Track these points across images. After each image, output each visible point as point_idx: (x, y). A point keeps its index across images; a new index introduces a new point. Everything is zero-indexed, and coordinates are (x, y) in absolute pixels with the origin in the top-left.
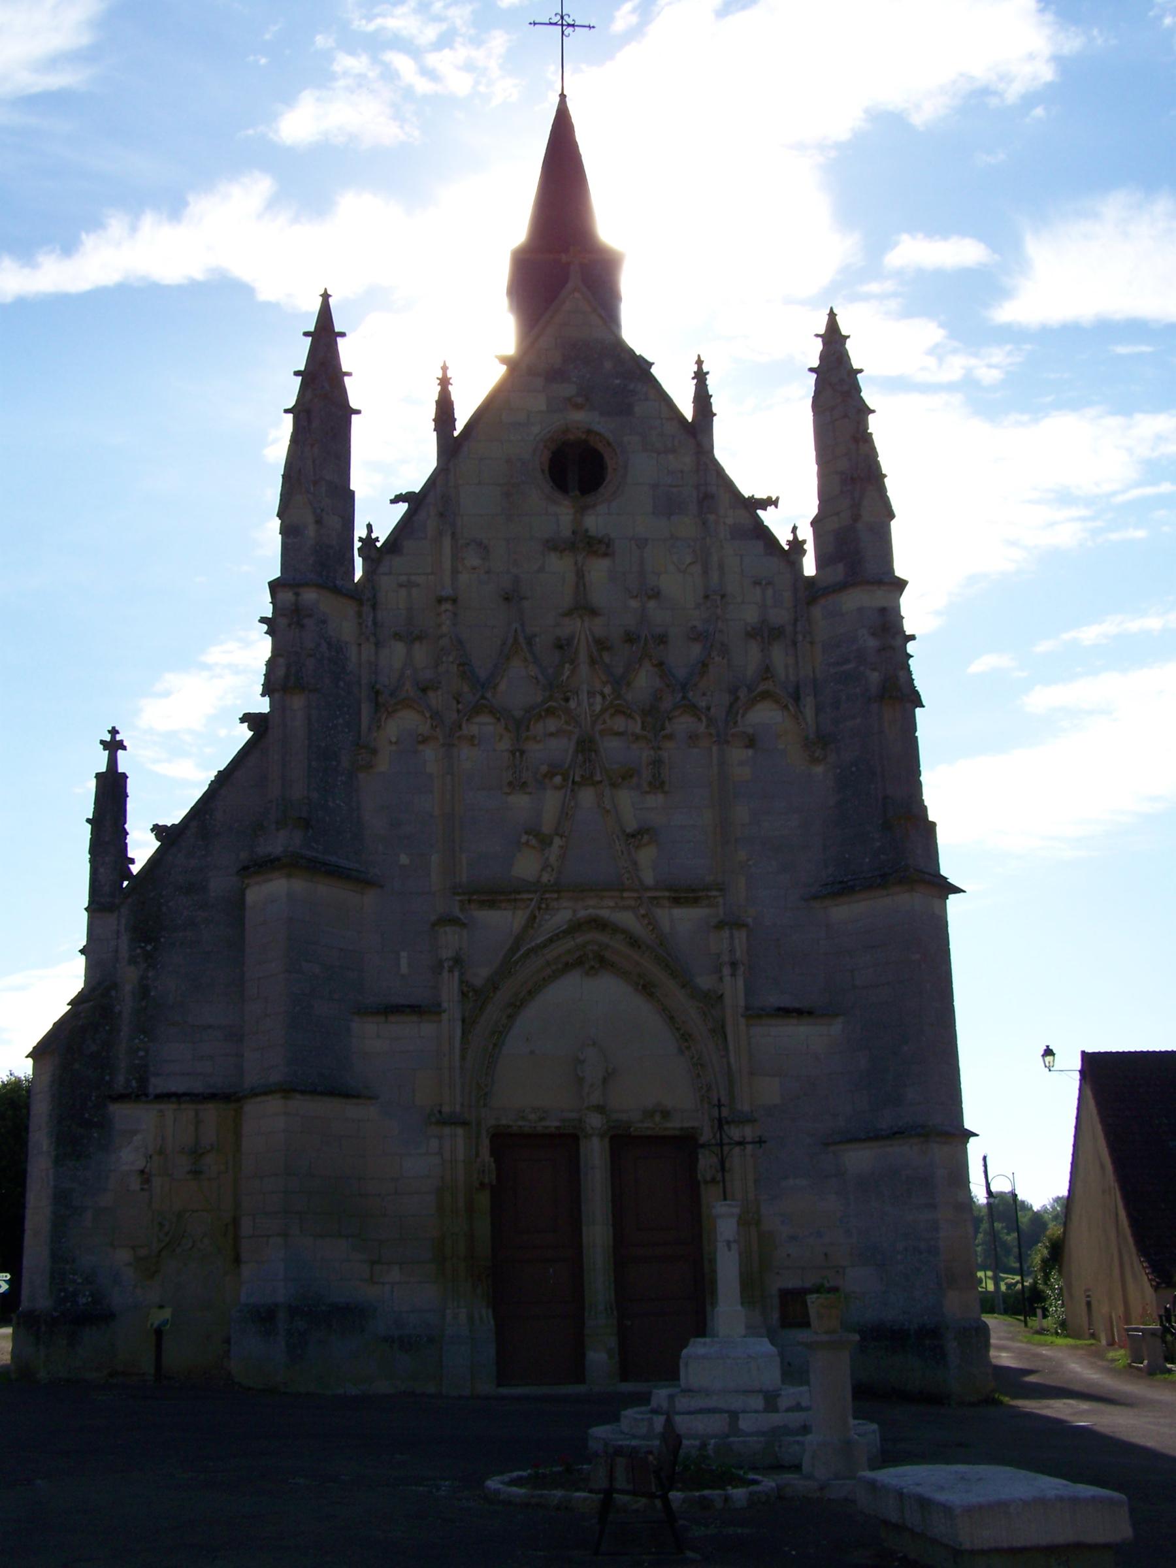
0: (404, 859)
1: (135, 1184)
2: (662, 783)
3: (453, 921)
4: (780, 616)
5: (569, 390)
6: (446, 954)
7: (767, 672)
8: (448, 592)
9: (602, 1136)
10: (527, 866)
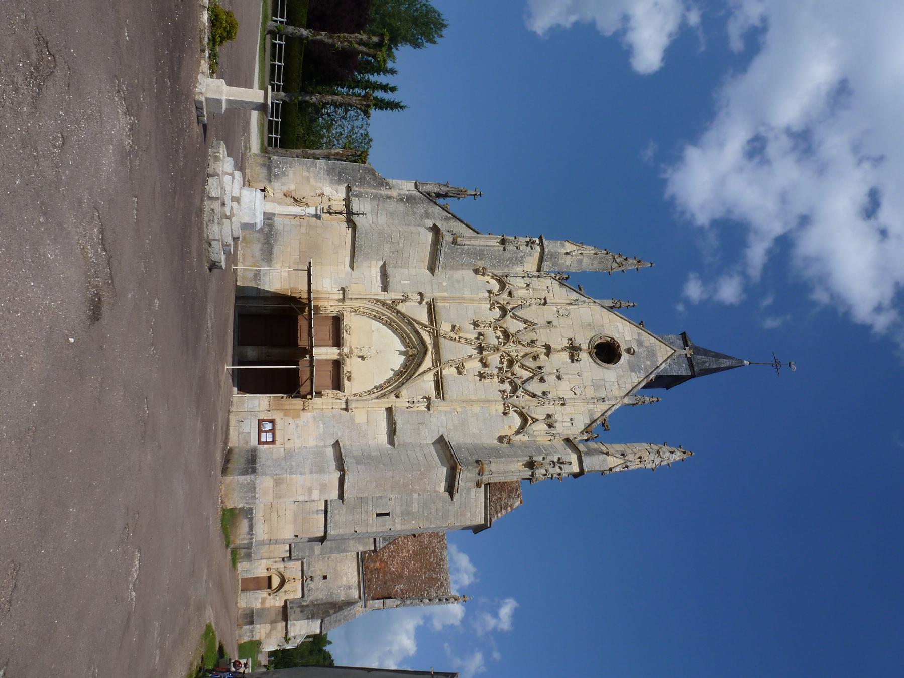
0: (445, 284)
1: (319, 192)
2: (485, 377)
3: (422, 299)
5: (636, 348)
6: (410, 294)
7: (535, 421)
8: (548, 301)
9: (340, 354)
10: (445, 328)
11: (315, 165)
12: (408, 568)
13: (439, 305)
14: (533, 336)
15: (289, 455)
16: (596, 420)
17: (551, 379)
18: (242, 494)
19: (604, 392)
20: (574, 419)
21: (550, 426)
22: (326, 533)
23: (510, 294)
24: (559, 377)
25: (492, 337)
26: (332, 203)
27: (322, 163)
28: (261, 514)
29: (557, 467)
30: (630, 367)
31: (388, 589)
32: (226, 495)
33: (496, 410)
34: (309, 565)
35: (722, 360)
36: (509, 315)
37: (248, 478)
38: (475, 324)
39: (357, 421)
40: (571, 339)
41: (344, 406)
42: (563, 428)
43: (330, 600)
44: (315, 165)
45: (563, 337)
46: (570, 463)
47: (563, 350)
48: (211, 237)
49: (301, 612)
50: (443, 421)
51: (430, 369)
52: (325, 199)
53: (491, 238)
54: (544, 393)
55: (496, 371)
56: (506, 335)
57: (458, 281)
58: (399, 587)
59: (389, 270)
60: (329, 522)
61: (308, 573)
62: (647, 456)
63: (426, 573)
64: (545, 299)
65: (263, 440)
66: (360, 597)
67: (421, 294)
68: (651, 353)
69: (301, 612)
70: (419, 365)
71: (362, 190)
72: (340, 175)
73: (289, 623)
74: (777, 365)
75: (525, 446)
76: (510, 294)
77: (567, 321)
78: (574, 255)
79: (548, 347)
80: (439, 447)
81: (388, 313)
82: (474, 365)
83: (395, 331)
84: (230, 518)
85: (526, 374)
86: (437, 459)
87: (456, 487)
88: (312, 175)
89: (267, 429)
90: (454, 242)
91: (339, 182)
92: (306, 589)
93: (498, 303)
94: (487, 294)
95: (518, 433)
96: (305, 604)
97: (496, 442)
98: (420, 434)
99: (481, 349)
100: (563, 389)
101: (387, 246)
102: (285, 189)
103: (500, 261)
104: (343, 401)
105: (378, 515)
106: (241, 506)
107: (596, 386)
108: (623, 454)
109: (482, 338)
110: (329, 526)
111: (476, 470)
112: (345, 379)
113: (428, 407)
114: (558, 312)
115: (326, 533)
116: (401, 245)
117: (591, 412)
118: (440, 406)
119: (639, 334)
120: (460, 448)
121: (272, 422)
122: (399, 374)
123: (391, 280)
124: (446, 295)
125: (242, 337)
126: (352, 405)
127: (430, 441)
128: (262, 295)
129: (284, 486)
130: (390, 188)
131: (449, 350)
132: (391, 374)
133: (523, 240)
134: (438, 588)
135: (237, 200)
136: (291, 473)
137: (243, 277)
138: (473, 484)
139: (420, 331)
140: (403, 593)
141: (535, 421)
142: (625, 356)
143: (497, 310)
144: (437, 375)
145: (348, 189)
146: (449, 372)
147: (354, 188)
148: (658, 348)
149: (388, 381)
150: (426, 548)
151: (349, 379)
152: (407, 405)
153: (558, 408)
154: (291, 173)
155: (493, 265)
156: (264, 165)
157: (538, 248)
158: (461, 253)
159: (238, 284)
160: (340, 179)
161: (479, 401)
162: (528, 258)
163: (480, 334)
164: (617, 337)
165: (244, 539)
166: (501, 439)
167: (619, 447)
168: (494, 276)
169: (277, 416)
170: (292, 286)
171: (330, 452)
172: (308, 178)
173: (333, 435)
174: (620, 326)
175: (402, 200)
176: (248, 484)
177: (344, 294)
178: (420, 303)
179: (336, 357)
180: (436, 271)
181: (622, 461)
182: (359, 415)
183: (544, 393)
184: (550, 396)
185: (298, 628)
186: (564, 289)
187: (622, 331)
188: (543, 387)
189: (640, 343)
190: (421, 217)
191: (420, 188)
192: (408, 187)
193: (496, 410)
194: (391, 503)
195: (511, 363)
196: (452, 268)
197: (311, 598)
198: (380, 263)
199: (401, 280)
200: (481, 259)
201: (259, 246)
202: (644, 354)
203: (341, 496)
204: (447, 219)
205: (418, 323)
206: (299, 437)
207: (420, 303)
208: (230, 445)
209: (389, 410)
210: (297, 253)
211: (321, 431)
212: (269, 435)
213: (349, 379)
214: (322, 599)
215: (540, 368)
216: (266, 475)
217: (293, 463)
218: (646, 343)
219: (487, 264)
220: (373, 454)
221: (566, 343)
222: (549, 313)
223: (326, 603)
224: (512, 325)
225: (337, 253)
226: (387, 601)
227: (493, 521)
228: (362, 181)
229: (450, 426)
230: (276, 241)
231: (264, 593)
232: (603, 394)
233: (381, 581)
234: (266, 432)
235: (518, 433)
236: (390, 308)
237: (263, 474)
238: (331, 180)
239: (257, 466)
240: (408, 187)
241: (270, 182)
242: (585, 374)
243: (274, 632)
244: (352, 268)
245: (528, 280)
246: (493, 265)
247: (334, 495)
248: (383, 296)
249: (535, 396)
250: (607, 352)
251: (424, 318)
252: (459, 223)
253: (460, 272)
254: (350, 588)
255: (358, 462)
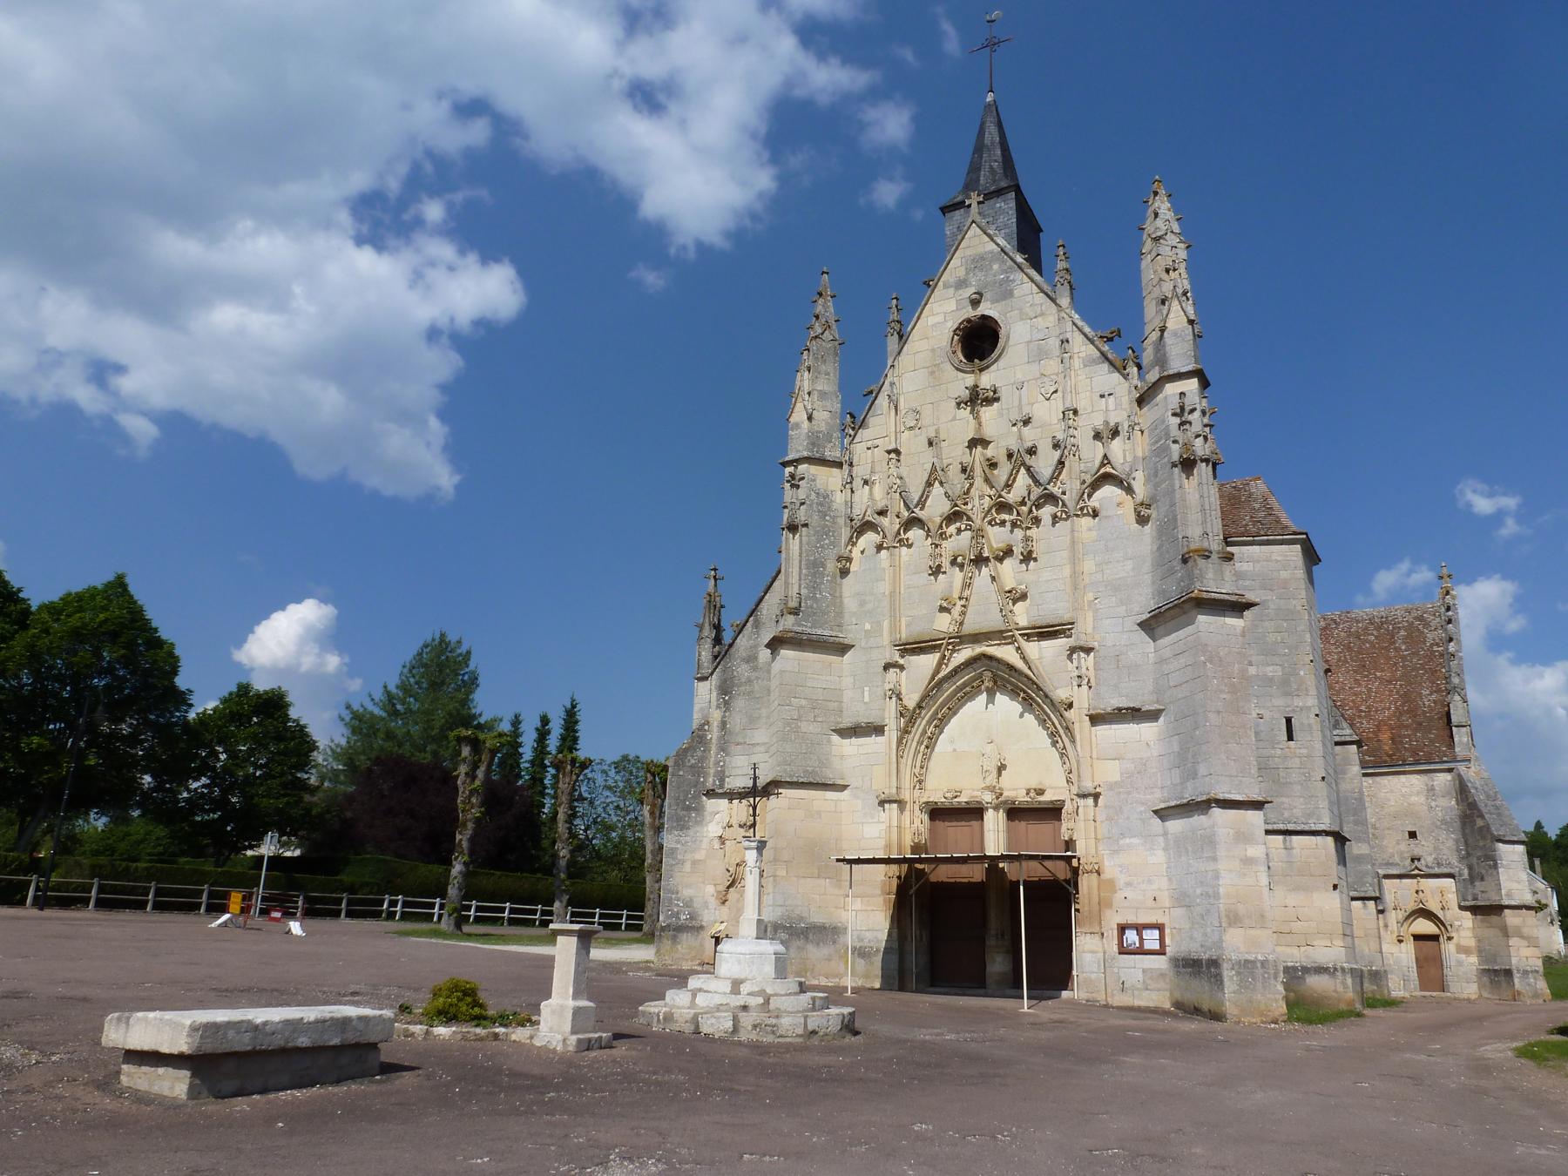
0: (867, 626)
1: (717, 845)
2: (1031, 552)
3: (895, 665)
4: (1118, 416)
5: (969, 292)
6: (888, 687)
7: (1106, 460)
8: (892, 446)
9: (996, 808)
11: (673, 851)
12: (1390, 682)
13: (904, 636)
14: (954, 470)
15: (1182, 900)
16: (1102, 353)
17: (1030, 435)
18: (1259, 985)
19: (1050, 341)
20: (1102, 392)
21: (1115, 433)
22: (1327, 833)
23: (882, 513)
24: (1026, 422)
25: (958, 542)
26: (734, 822)
27: (669, 840)
28: (1295, 951)
29: (1190, 418)
30: (1004, 298)
31: (1431, 719)
32: (1261, 1014)
33: (1090, 529)
34: (1388, 864)
35: (987, 141)
36: (918, 513)
37: (1227, 974)
38: (936, 571)
39: (1117, 778)
40: (958, 404)
41: (1090, 801)
42: (1119, 408)
43: (1457, 825)
44: (673, 851)
45: (954, 419)
46: (1182, 394)
47: (977, 417)
48: (800, 1031)
49: (1482, 879)
50: (1112, 623)
51: (1018, 648)
52: (728, 833)
53: (788, 549)
54: (1056, 446)
55: (1019, 533)
56: (954, 517)
57: (862, 604)
58: (1428, 698)
59: (847, 722)
60: (1306, 828)
61: (1406, 866)
62: (1165, 261)
63: (1397, 650)
64: (889, 452)
65: (1156, 946)
66: (1450, 770)
67: (887, 667)
68: (978, 263)
69: (1482, 879)
70: (1011, 668)
71: (712, 771)
72: (688, 809)
73: (1506, 902)
74: (992, 44)
75: (1152, 476)
76: (882, 513)
77: (927, 412)
78: (812, 405)
79: (973, 443)
80: (1159, 630)
81: (921, 724)
82: (1009, 571)
83: (953, 711)
84: (1305, 1008)
85: (1022, 479)
86: (1181, 634)
87: (1234, 598)
88: (688, 856)
89: (1136, 939)
90: (795, 612)
91: (699, 809)
92: (1437, 870)
93: (898, 533)
94: (884, 552)
95: (1129, 490)
96: (1466, 872)
97: (1148, 528)
98: (1139, 665)
99: (980, 561)
100: (1048, 414)
101: (805, 727)
102: (713, 902)
103: (826, 532)
104: (1081, 802)
105: (1290, 738)
106: (1281, 988)
107: (1040, 355)
108: (1163, 302)
109: (960, 560)
110: (1314, 828)
111: (1201, 562)
112: (1041, 798)
113: (1088, 650)
114: (911, 428)
115: (1327, 833)
116: (804, 702)
117: (1089, 362)
118: (1085, 630)
119: (946, 286)
120: (1161, 593)
121: (1122, 929)
122: (1028, 703)
123: (864, 719)
124: (886, 624)
125: (971, 979)
126: (1088, 786)
127: (1150, 645)
128: (896, 945)
129: (1241, 909)
130: (708, 723)
131: (983, 615)
132: (1029, 718)
133: (789, 495)
134: (1427, 625)
135: (736, 985)
136: (1217, 896)
137: (866, 976)
138: (1227, 567)
139: (951, 667)
140: (1438, 691)
141: (1106, 460)
142: (986, 309)
143: (910, 534)
144: (1028, 637)
145: (711, 794)
146: (1022, 615)
147: (709, 785)
148: (969, 252)
149: (1042, 722)
150: (1349, 649)
151: (1041, 792)
152: (1085, 688)
153: (1081, 421)
154: (687, 893)
155: (832, 543)
156: (674, 938)
157: (803, 468)
158: (814, 598)
159: (877, 985)
160: (695, 809)
161: (1074, 560)
162: (819, 484)
163: (954, 562)
164: (952, 324)
165: (1344, 983)
166: (1142, 520)
167: (1150, 309)
168: (852, 542)
169: (1112, 920)
170: (879, 892)
171: (1176, 825)
172: (694, 863)
173: (1143, 821)
174: (932, 320)
175: (726, 703)
176: (1238, 974)
177: (890, 802)
178: (902, 668)
179: (1002, 814)
180: (846, 641)
181: (1175, 303)
182: (1105, 773)
183: (1056, 446)
184: (1060, 436)
185: (1515, 886)
186: (871, 421)
187: (941, 316)
188: (1045, 447)
189: (961, 284)
190: (755, 669)
191: (706, 672)
192: (705, 692)
193: (1090, 529)
194: (1267, 714)
195: (1003, 507)
196: (840, 614)
197: (1455, 862)
198: (835, 738)
199: (864, 702)
200: (824, 566)
201: (811, 948)
202: (980, 275)
203: (1257, 805)
204: (757, 625)
205: (937, 672)
206: (1150, 881)
207: (902, 668)
208: (1167, 1005)
209: (1095, 719)
210: (822, 881)
211: (1135, 841)
212: (1147, 934)
213: (1041, 792)
214: (1457, 841)
215: (1010, 456)
216: (1221, 941)
217: (1198, 891)
218: (961, 273)
219: (831, 554)
220: (1176, 748)
221: (965, 413)
222: (913, 444)
223: (1464, 835)
224: (937, 506)
225: (819, 813)
226: (1454, 719)
227: (1294, 528)
228: (698, 770)
229: (1122, 610)
230: (801, 919)
231: (1449, 949)
232: (1054, 343)
233: (1416, 730)
234: (1141, 940)
235: (1129, 490)
236: (911, 721)
237: (1221, 947)
238: (699, 823)
239: (1205, 957)
240: (705, 692)
241: (702, 927)
242: (1020, 376)
243: (1526, 931)
244: (844, 787)
245: (858, 483)
246: (832, 543)
247: (1255, 818)
248: (892, 734)
249: (1061, 463)
250: (979, 340)
251: (931, 660)
252: (764, 605)
253: (846, 601)
254: (1431, 789)
255: (1193, 775)
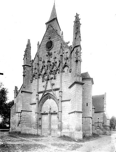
25: (46, 77)
41: (60, 112)
82: (53, 81)
83: (45, 101)
131: (49, 87)
151: (55, 111)
205: (43, 96)
236: (39, 103)
248: (37, 104)
